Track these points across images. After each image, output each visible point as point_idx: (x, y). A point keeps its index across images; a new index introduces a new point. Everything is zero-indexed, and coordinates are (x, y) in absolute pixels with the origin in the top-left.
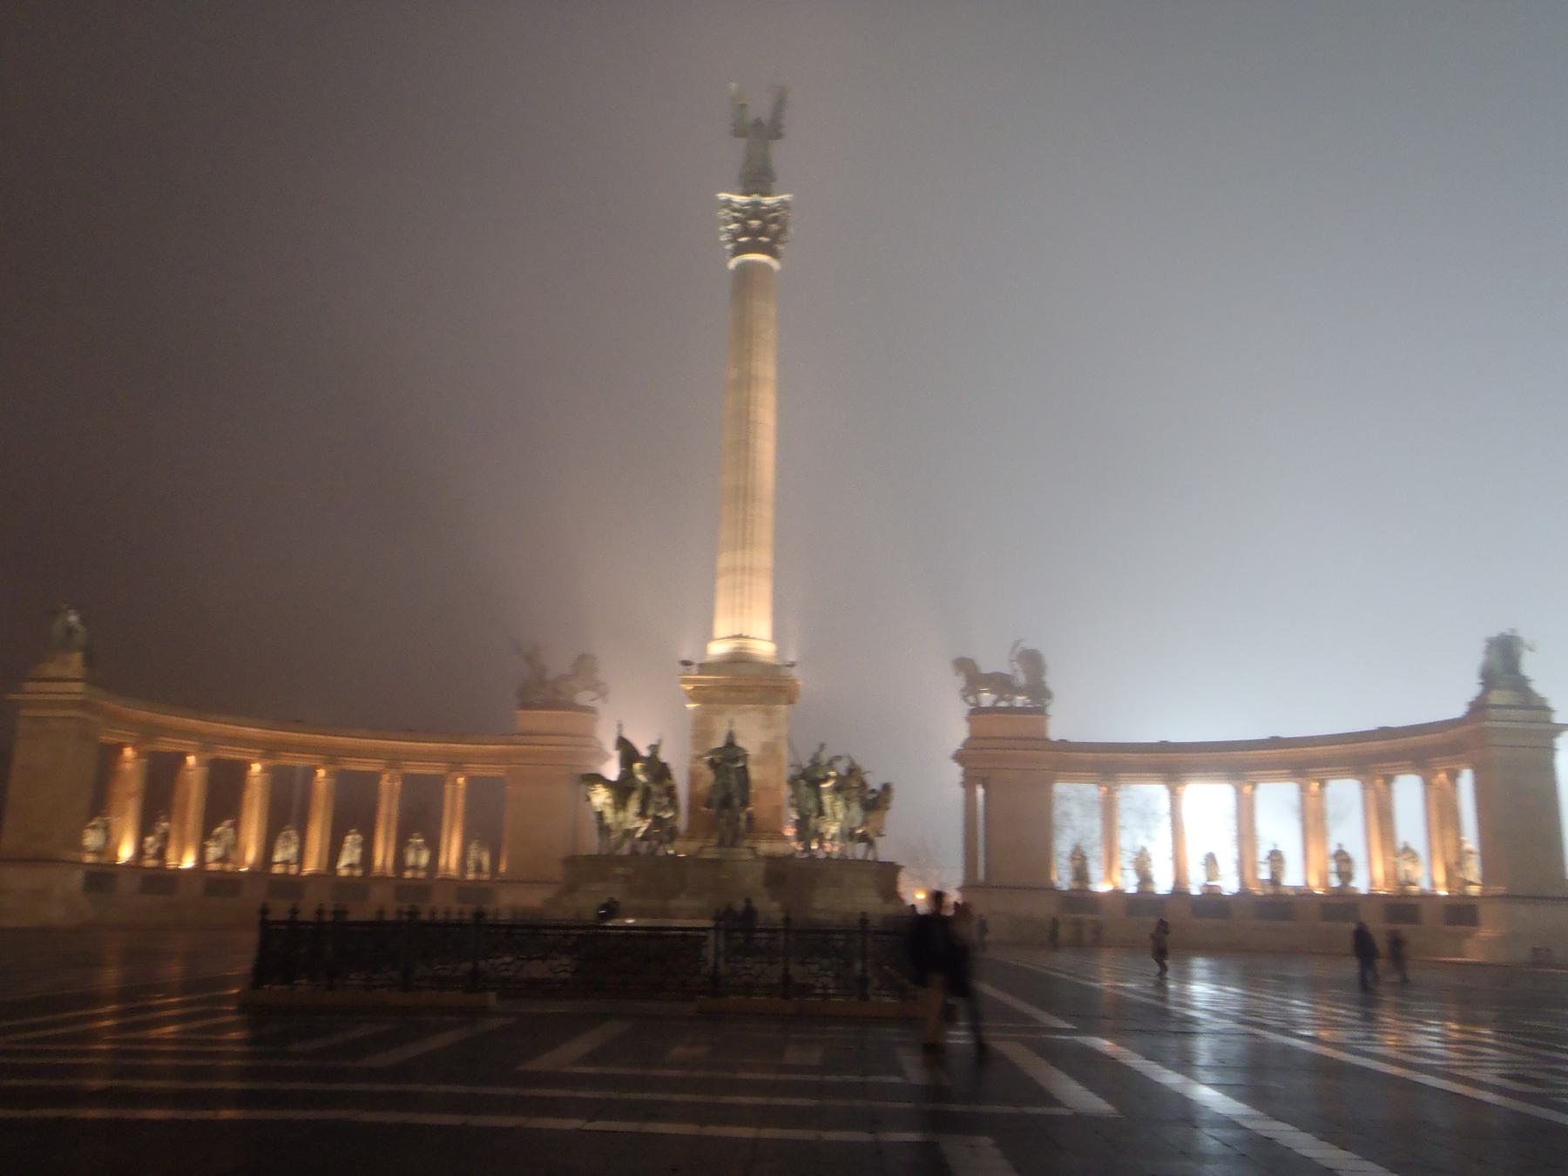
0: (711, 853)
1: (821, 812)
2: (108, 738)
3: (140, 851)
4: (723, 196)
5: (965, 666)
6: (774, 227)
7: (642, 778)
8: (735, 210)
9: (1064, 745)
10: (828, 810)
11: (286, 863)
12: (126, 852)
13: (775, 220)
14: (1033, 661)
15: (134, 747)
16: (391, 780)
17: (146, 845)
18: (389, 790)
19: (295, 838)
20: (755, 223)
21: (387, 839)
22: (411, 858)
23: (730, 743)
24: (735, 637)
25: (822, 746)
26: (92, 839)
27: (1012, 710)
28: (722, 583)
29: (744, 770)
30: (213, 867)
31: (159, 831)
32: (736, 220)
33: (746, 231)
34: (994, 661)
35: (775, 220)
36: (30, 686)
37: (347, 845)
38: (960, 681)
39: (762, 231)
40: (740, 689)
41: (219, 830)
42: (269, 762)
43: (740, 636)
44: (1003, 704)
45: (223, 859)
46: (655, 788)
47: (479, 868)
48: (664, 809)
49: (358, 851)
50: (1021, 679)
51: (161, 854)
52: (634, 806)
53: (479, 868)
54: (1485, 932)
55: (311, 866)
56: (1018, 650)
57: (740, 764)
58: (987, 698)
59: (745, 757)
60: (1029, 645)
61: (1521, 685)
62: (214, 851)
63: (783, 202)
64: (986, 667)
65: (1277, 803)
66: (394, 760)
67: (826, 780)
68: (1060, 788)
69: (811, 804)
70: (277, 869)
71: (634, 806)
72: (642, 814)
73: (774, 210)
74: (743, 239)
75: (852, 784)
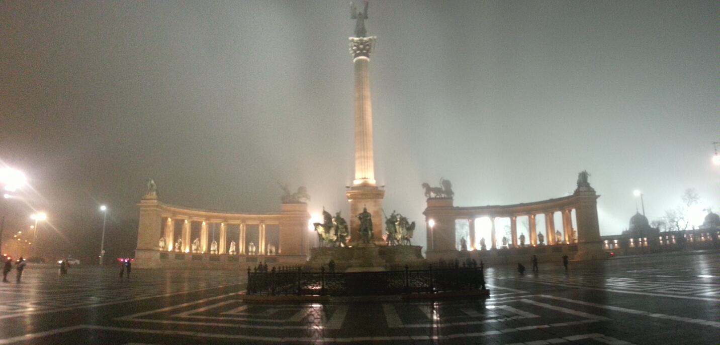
0: (361, 246)
1: (396, 231)
2: (164, 215)
3: (174, 247)
4: (351, 38)
5: (426, 186)
6: (368, 47)
7: (335, 223)
8: (354, 42)
9: (458, 208)
10: (398, 231)
11: (214, 251)
12: (170, 248)
13: (368, 45)
14: (447, 184)
15: (171, 218)
16: (243, 226)
17: (176, 246)
18: (242, 228)
19: (216, 243)
20: (361, 46)
21: (243, 243)
22: (250, 249)
24: (363, 178)
25: (394, 211)
26: (161, 244)
27: (442, 198)
28: (357, 162)
29: (370, 219)
30: (194, 252)
31: (179, 241)
32: (355, 46)
33: (358, 49)
34: (435, 184)
35: (368, 45)
37: (231, 245)
38: (424, 190)
39: (364, 49)
41: (195, 241)
42: (208, 222)
43: (365, 178)
44: (438, 197)
45: (197, 249)
46: (340, 226)
48: (344, 233)
49: (235, 247)
50: (444, 189)
51: (179, 248)
52: (332, 232)
55: (221, 251)
56: (442, 180)
57: (369, 218)
58: (433, 195)
59: (370, 215)
60: (446, 178)
61: (588, 185)
62: (194, 247)
63: (370, 39)
64: (432, 186)
65: (522, 222)
66: (243, 221)
67: (397, 221)
68: (457, 221)
69: (393, 229)
70: (212, 252)
71: (332, 232)
72: (336, 234)
73: (368, 42)
74: (358, 52)
75: (403, 221)
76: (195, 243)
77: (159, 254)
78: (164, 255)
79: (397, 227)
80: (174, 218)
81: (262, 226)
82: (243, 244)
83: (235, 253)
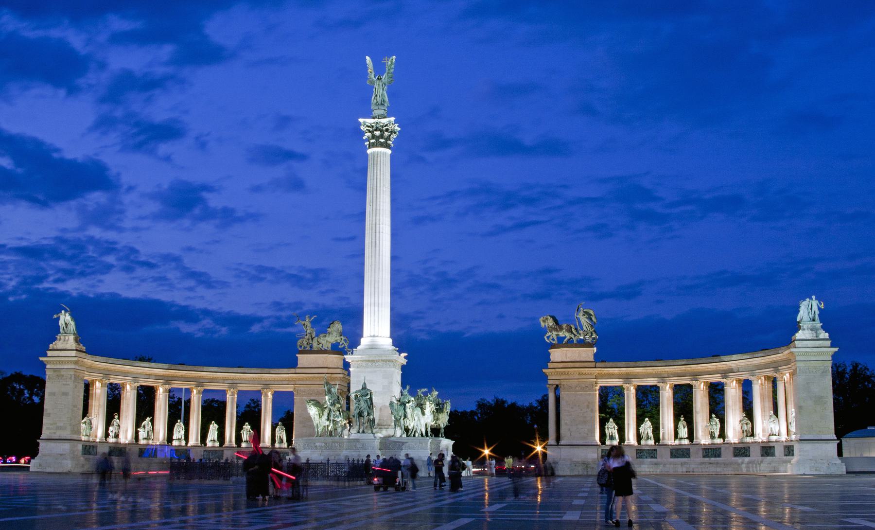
1: (405, 417)
2: (86, 378)
3: (107, 435)
10: (409, 415)
11: (179, 439)
16: (233, 394)
20: (377, 133)
23: (364, 388)
29: (371, 399)
30: (142, 442)
35: (387, 130)
36: (49, 353)
39: (382, 136)
40: (373, 361)
42: (168, 387)
43: (374, 336)
45: (147, 438)
47: (281, 441)
51: (117, 436)
53: (281, 441)
54: (794, 459)
62: (142, 434)
69: (401, 413)
72: (328, 419)
74: (372, 141)
76: (144, 427)
77: (80, 447)
78: (89, 449)
79: (408, 411)
80: (107, 382)
81: (266, 395)
82: (231, 427)
83: (217, 444)
